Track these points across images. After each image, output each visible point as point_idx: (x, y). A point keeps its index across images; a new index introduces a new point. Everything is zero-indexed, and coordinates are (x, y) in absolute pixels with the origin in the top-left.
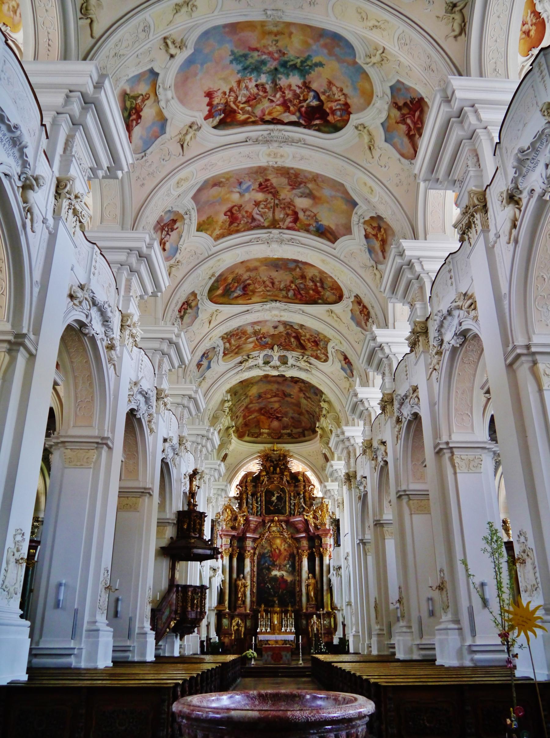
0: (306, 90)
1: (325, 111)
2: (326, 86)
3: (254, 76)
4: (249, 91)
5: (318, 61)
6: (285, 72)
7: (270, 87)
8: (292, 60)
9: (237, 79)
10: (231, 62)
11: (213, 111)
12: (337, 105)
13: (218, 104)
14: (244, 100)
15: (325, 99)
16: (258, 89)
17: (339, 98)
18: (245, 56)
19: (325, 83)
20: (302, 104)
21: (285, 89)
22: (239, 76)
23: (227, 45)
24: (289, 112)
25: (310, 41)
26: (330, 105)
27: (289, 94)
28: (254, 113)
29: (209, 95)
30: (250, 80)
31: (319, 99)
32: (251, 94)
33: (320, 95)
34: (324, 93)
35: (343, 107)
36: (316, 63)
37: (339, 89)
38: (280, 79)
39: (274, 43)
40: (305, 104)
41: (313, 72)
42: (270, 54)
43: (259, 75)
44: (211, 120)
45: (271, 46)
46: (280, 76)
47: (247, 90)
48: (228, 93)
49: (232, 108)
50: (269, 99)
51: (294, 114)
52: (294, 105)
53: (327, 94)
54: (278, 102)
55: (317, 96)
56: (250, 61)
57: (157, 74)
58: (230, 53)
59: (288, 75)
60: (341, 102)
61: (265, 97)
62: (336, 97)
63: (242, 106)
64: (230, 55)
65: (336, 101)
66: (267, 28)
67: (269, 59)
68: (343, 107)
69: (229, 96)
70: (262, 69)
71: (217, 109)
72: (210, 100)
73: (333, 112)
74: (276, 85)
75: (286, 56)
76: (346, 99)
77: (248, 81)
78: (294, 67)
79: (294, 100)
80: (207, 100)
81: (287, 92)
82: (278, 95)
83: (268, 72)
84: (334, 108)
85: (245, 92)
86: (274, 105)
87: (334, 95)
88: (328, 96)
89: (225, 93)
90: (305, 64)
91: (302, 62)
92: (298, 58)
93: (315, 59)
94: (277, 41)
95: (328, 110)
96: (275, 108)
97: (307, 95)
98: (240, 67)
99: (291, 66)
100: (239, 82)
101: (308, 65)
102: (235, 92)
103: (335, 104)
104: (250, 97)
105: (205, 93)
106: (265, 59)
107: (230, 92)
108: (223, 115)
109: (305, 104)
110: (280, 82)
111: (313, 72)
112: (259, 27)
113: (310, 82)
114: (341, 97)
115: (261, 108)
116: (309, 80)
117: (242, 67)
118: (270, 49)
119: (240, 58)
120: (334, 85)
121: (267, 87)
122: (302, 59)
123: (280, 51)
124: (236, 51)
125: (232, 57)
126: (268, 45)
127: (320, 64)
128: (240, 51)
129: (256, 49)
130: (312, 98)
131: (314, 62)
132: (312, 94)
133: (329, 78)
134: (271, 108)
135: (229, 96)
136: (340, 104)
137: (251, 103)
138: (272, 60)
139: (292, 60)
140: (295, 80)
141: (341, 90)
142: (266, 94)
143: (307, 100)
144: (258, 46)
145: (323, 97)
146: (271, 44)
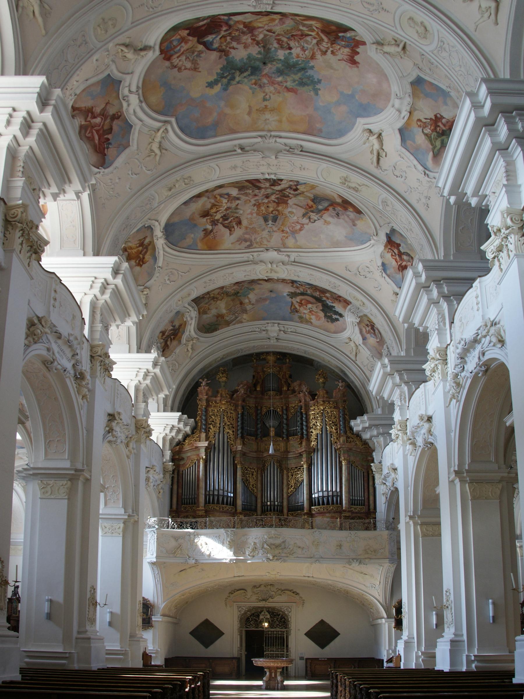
0: (224, 47)
1: (194, 37)
2: (199, 62)
3: (293, 60)
4: (301, 45)
5: (215, 87)
6: (253, 61)
7: (272, 45)
8: (245, 77)
9: (314, 61)
10: (319, 81)
11: (353, 44)
12: (180, 50)
13: (345, 47)
14: (308, 39)
15: (196, 47)
16: (288, 44)
17: (180, 58)
18: (302, 84)
19: (202, 64)
20: (227, 32)
21: (252, 44)
22: (312, 64)
23: (321, 104)
24: (245, 23)
25: (228, 111)
26: (190, 45)
27: (247, 39)
28: (296, 23)
29: (353, 62)
30: (298, 56)
31: (204, 44)
32: (298, 42)
33: (204, 49)
34: (200, 52)
35: (172, 52)
36: (217, 85)
37: (183, 68)
38: (259, 53)
39: (268, 97)
40: (223, 33)
41: (219, 71)
42: (273, 83)
43: (287, 59)
44: (357, 38)
45: (271, 92)
46: (259, 56)
47: (303, 47)
48: (329, 52)
49: (327, 36)
50: (274, 33)
51: (238, 22)
52: (237, 30)
53: (196, 54)
54: (260, 30)
55: (208, 46)
56: (297, 77)
57: (401, 131)
58: (320, 92)
59: (249, 57)
60: (175, 56)
61: (278, 35)
62: (183, 58)
63: (313, 34)
64: (320, 89)
65: (183, 53)
66: (276, 118)
67: (273, 75)
68: (172, 52)
69: (328, 48)
70: (283, 65)
71: (346, 43)
72: (354, 57)
73: (183, 40)
74: (264, 47)
75: (253, 81)
76: (171, 63)
77: (301, 55)
78: (242, 70)
79: (239, 35)
80: (357, 58)
81: (250, 40)
82: (261, 36)
83: (274, 60)
84: (183, 44)
85: (306, 45)
86: (266, 27)
87: (187, 58)
88: (193, 53)
89: (333, 53)
90: (229, 78)
91: (233, 79)
92: (238, 83)
93: (218, 88)
94: (265, 99)
95: (191, 38)
96: (265, 25)
97: (221, 43)
98: (310, 72)
99: (246, 70)
100: (313, 57)
101: (225, 77)
102: (320, 49)
103: (182, 50)
104: (301, 39)
105: (358, 67)
106: (279, 77)
107: (326, 51)
108: (340, 35)
109: (223, 33)
110: (259, 49)
111: (219, 71)
112: (284, 119)
113: (220, 57)
114: (178, 61)
115: (284, 25)
116: (221, 60)
117: (307, 72)
118: (272, 89)
119: (308, 82)
120: (189, 69)
121: (276, 45)
122: (234, 82)
123: (260, 86)
124: (312, 93)
125: (317, 87)
126: (274, 94)
127: (211, 85)
128: (306, 91)
129: (288, 90)
130: (215, 41)
131: (220, 85)
132: (216, 46)
133: (199, 74)
134: (270, 24)
135: (328, 48)
136: (176, 53)
137: (299, 33)
138: (270, 75)
139: (245, 77)
140: (240, 54)
141: (180, 70)
142: (278, 38)
143: (221, 38)
144: (286, 94)
145: (201, 47)
146: (271, 95)
